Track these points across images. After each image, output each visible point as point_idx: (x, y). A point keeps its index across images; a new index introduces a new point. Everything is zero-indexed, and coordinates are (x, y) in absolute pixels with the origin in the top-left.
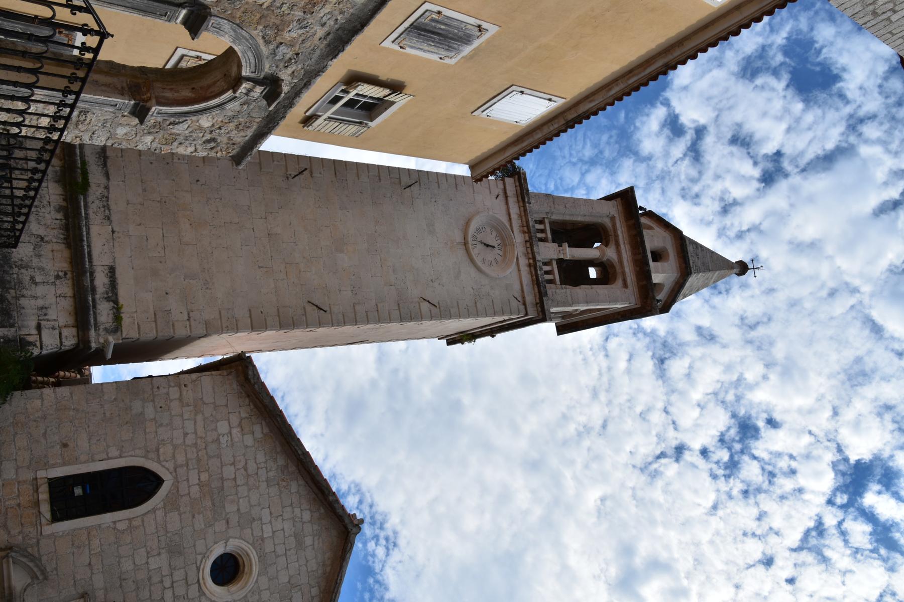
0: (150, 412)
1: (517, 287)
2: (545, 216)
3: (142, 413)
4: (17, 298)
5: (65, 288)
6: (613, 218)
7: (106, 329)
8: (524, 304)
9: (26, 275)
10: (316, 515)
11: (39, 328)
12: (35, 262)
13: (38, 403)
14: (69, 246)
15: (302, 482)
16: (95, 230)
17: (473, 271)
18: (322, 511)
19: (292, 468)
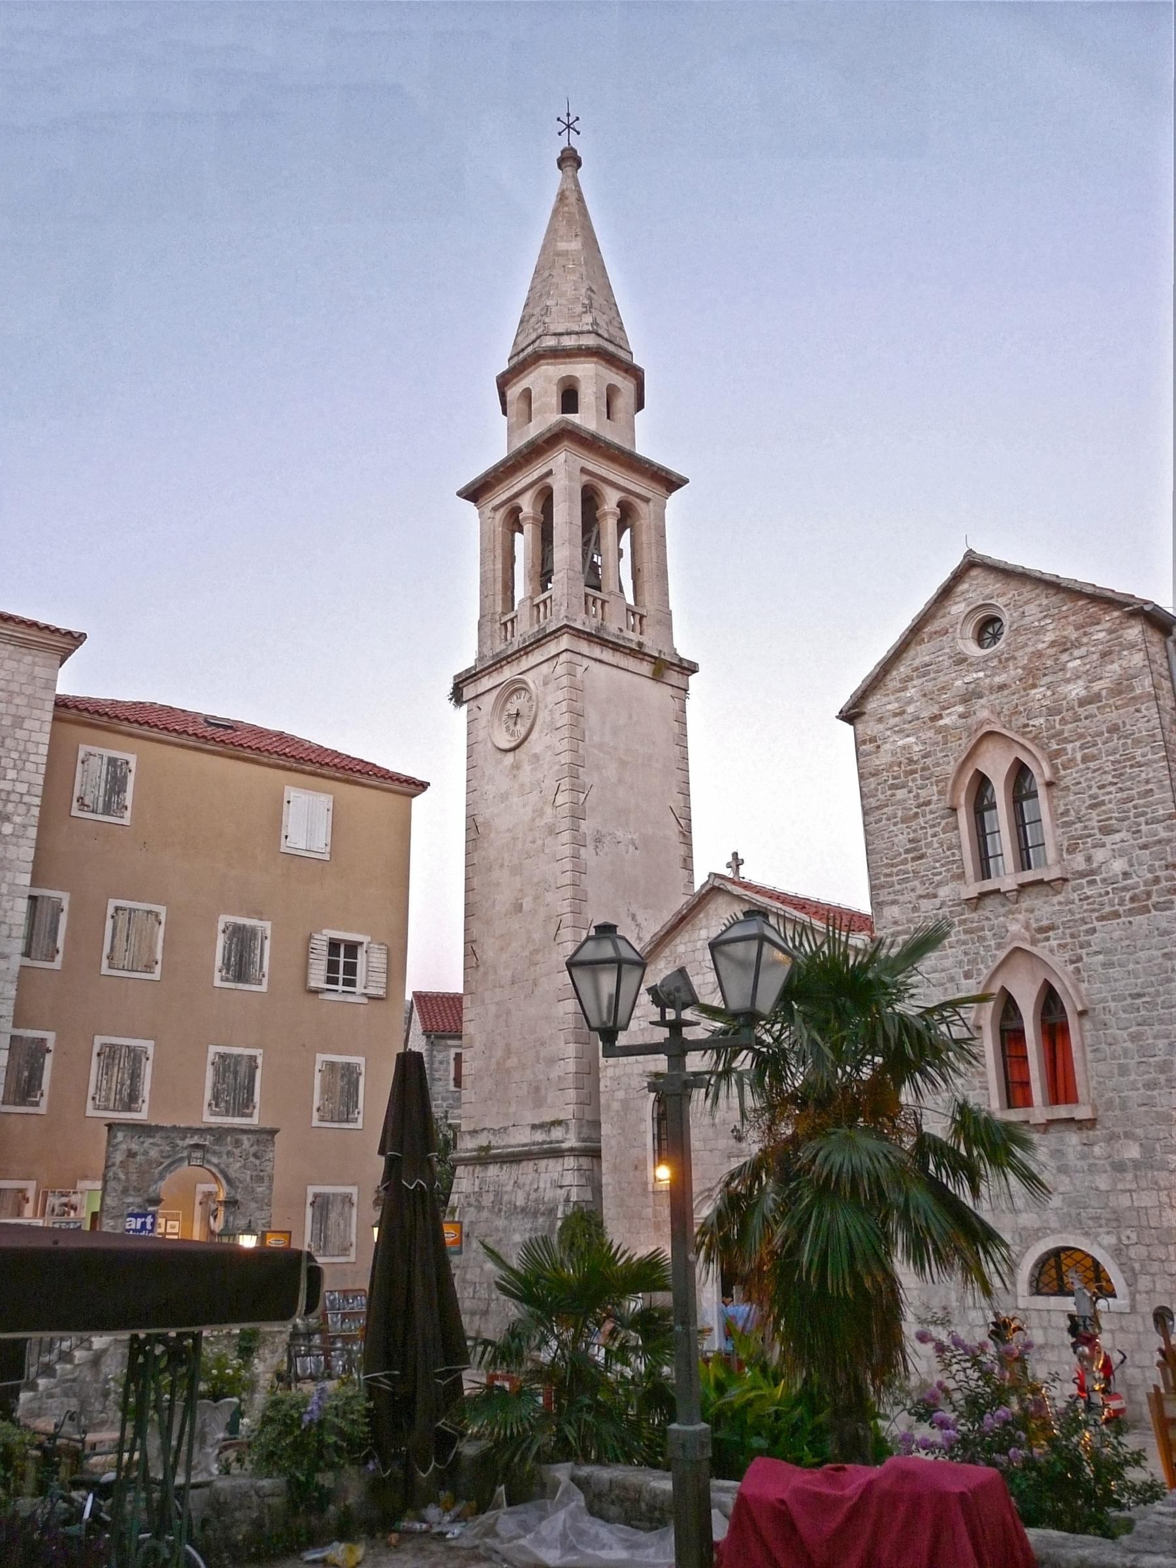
0: (620, 1095)
1: (545, 669)
2: (498, 625)
3: (622, 1101)
4: (544, 1203)
5: (543, 1164)
6: (495, 509)
7: (567, 1132)
8: (558, 655)
9: (533, 1196)
10: (704, 923)
11: (561, 1187)
12: (527, 1188)
13: (610, 1188)
14: (521, 1161)
15: (678, 940)
16: (513, 1141)
17: (534, 736)
18: (702, 915)
19: (667, 952)
